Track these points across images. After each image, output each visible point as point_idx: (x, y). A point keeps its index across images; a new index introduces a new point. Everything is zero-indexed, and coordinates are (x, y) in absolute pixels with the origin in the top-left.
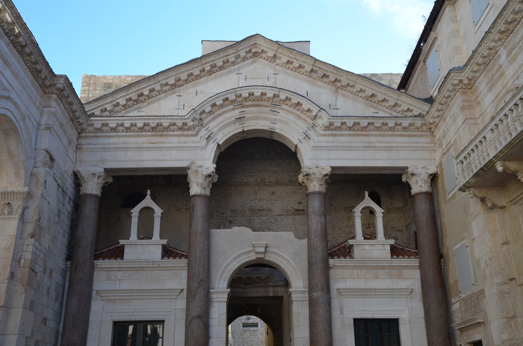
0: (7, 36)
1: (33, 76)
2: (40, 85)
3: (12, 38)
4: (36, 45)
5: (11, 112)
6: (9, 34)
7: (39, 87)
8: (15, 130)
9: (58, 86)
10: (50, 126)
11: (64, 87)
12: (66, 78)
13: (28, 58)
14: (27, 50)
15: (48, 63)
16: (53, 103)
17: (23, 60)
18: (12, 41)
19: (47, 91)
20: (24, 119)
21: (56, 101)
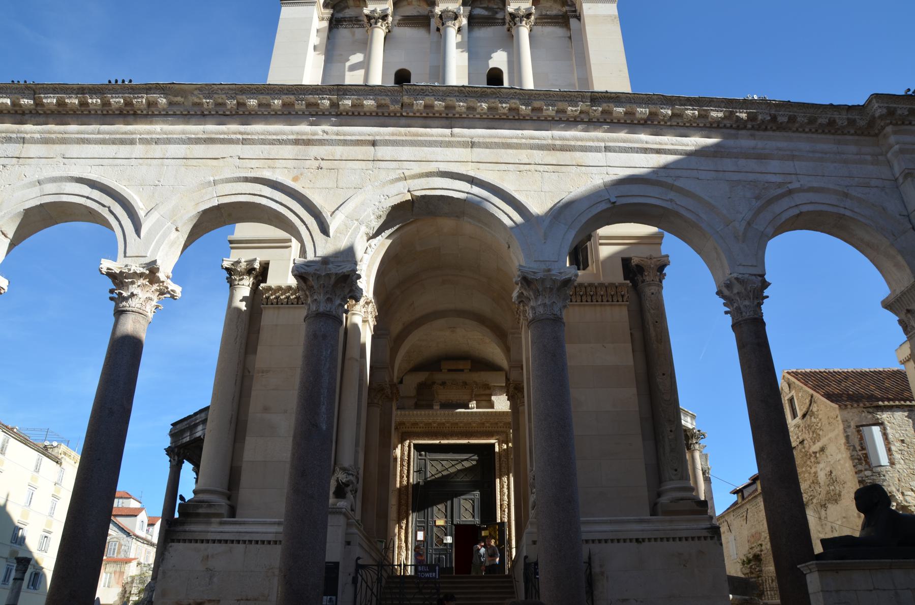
0: (742, 129)
1: (833, 134)
2: (856, 134)
3: (749, 126)
4: (788, 105)
5: (811, 203)
6: (741, 126)
7: (856, 137)
8: (842, 217)
9: (877, 114)
10: (907, 171)
11: (888, 108)
12: (877, 96)
13: (797, 125)
14: (783, 119)
15: (831, 105)
16: (892, 139)
17: (794, 132)
18: (753, 128)
19: (877, 131)
20: (846, 195)
21: (895, 133)
